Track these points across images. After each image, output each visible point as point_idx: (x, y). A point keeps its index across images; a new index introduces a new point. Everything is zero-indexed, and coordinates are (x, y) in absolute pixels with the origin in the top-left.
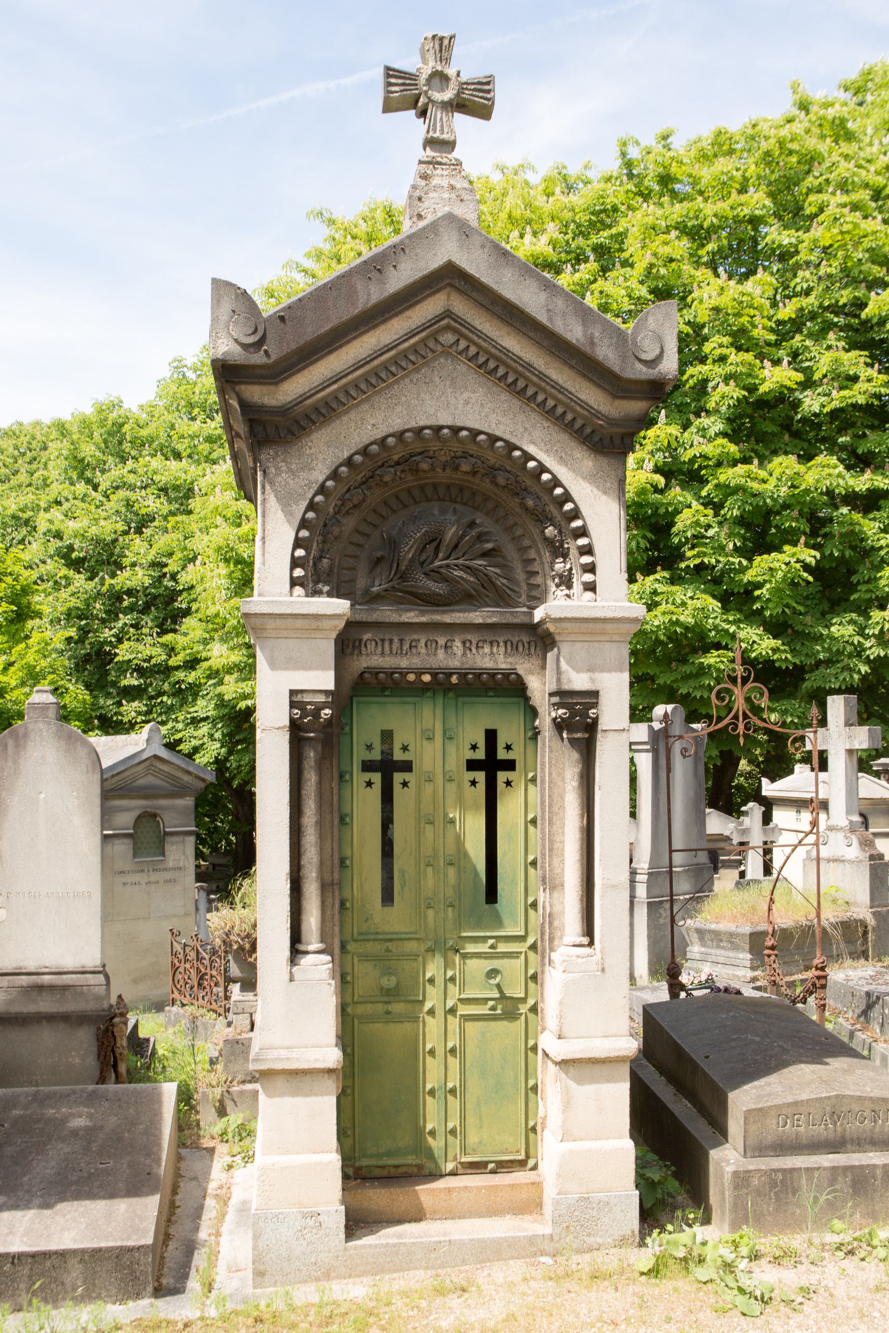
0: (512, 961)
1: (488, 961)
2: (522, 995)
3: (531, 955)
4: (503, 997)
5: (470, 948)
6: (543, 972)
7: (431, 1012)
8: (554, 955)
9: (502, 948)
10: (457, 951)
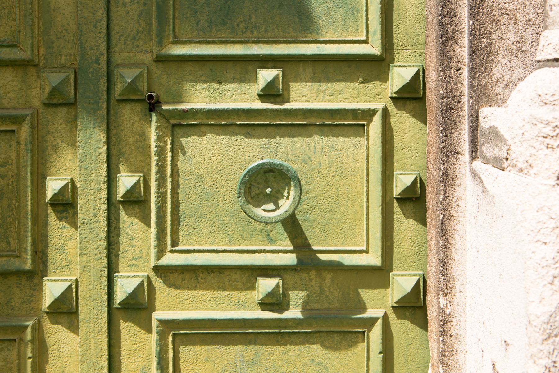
0: (341, 142)
1: (257, 143)
2: (373, 259)
3: (404, 123)
4: (308, 262)
5: (201, 97)
6: (447, 180)
7: (65, 310)
8: (490, 116)
9: (305, 96)
10: (153, 105)
